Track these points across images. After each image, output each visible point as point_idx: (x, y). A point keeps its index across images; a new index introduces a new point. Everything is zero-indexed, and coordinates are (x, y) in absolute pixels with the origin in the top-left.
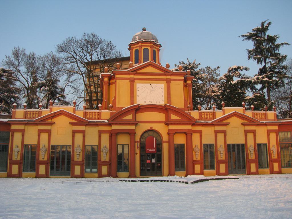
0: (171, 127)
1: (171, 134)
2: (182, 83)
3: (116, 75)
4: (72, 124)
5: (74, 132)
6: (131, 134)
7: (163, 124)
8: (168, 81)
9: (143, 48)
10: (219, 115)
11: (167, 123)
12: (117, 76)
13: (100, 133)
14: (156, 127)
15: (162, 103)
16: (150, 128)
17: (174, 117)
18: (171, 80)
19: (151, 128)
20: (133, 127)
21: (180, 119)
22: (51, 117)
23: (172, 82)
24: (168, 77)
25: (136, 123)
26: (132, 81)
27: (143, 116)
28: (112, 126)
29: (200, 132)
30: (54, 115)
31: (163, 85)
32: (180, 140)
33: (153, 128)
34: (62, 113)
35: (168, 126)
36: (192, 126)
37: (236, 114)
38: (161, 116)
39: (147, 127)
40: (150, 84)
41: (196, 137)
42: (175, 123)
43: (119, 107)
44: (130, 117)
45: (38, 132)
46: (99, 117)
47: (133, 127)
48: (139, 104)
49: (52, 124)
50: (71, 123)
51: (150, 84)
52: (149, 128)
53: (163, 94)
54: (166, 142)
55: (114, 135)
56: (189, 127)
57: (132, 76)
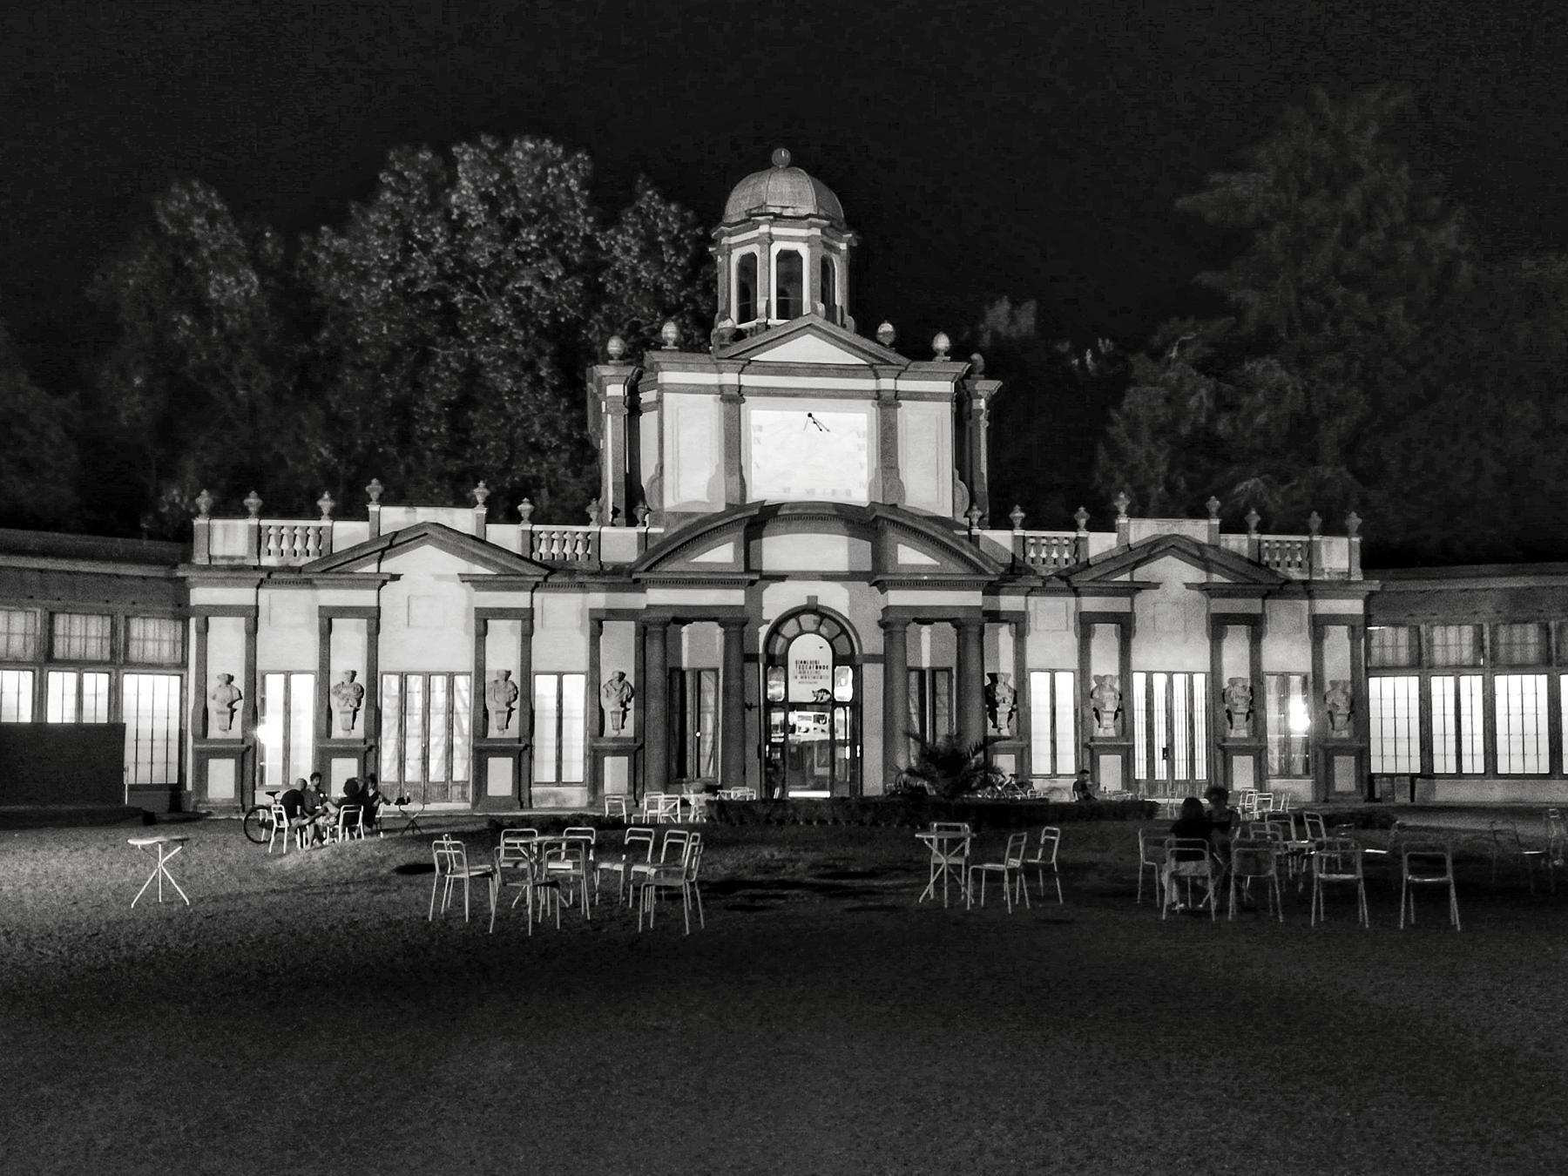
0: (897, 598)
3: (662, 371)
4: (478, 583)
5: (483, 619)
8: (887, 403)
9: (776, 248)
13: (598, 622)
14: (836, 597)
15: (860, 495)
16: (805, 603)
17: (909, 556)
18: (897, 396)
19: (814, 598)
20: (736, 597)
21: (932, 566)
22: (379, 553)
26: (733, 399)
27: (778, 550)
28: (649, 590)
30: (391, 542)
34: (426, 534)
35: (882, 593)
36: (983, 594)
40: (810, 415)
42: (914, 582)
44: (723, 554)
45: (320, 617)
46: (589, 552)
47: (736, 597)
48: (764, 501)
50: (466, 578)
51: (810, 415)
52: (804, 602)
53: (864, 459)
57: (730, 378)
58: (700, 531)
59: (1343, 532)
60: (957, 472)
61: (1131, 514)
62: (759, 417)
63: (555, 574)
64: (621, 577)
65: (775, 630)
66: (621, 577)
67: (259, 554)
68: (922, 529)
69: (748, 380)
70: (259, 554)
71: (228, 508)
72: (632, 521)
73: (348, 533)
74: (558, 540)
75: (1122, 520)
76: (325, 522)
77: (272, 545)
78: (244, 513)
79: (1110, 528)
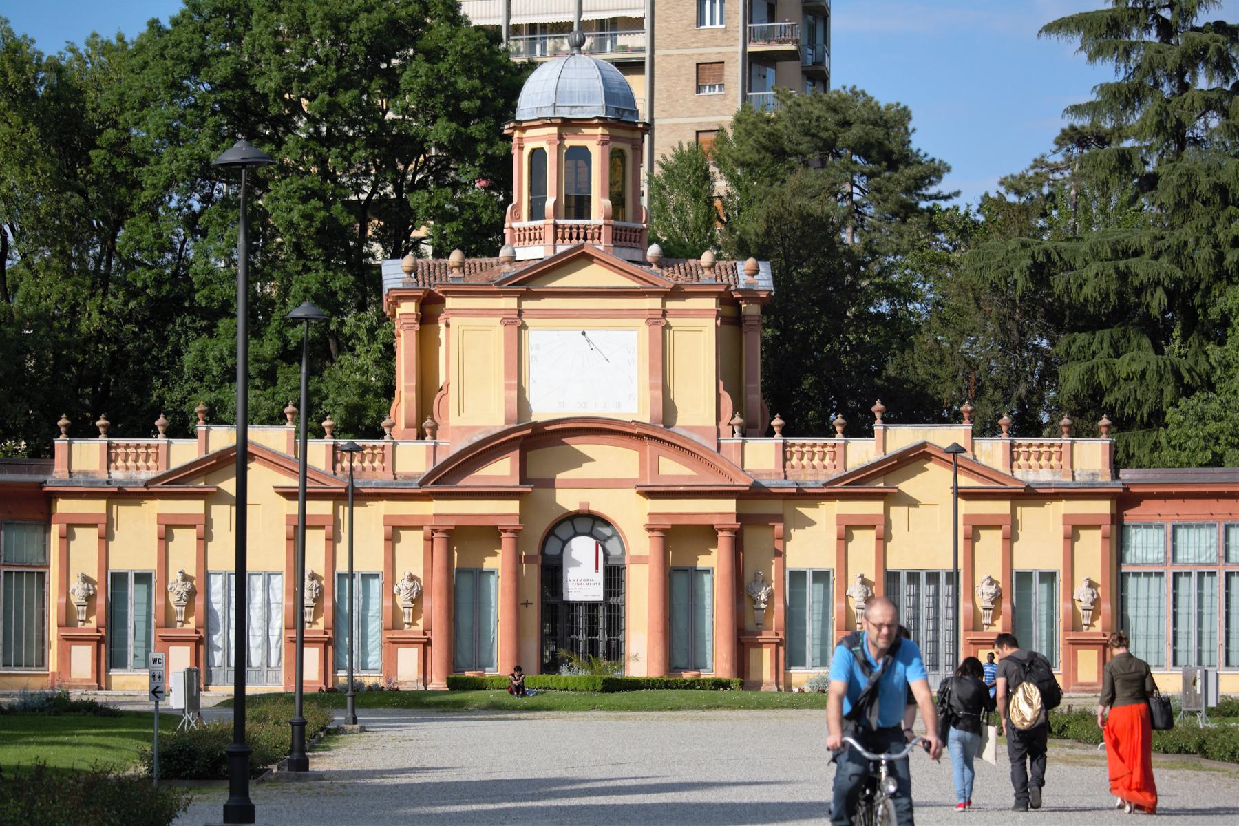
2: (710, 324)
7: (634, 491)
10: (862, 452)
12: (451, 303)
20: (513, 507)
21: (690, 477)
31: (633, 335)
33: (591, 508)
40: (584, 333)
43: (459, 428)
51: (584, 333)
54: (639, 560)
56: (730, 506)
59: (1093, 434)
60: (721, 383)
61: (886, 420)
62: (539, 338)
65: (551, 532)
67: (108, 468)
69: (526, 305)
70: (108, 468)
71: (83, 430)
72: (421, 436)
75: (878, 426)
76: (161, 440)
77: (120, 463)
78: (95, 434)
79: (870, 434)
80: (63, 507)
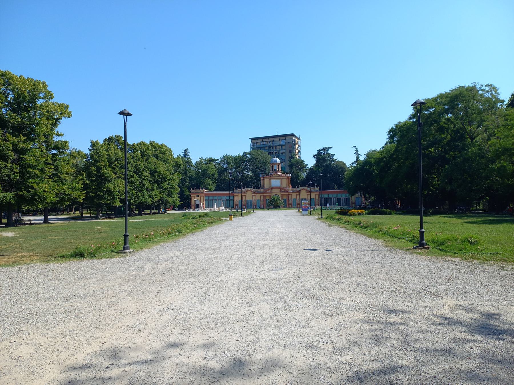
0: (282, 194)
1: (282, 196)
6: (270, 196)
8: (281, 179)
11: (281, 192)
12: (265, 178)
13: (261, 196)
14: (277, 193)
17: (283, 191)
20: (270, 194)
23: (283, 179)
24: (281, 178)
25: (271, 192)
26: (270, 179)
27: (273, 190)
29: (292, 195)
32: (285, 198)
37: (303, 189)
38: (279, 190)
39: (275, 194)
41: (290, 197)
47: (270, 194)
49: (246, 194)
55: (265, 196)
56: (288, 194)
57: (270, 178)
58: (268, 189)
63: (258, 193)
64: (262, 193)
66: (262, 193)
68: (283, 189)
69: (271, 178)
73: (244, 190)
74: (258, 190)
80: (235, 195)
